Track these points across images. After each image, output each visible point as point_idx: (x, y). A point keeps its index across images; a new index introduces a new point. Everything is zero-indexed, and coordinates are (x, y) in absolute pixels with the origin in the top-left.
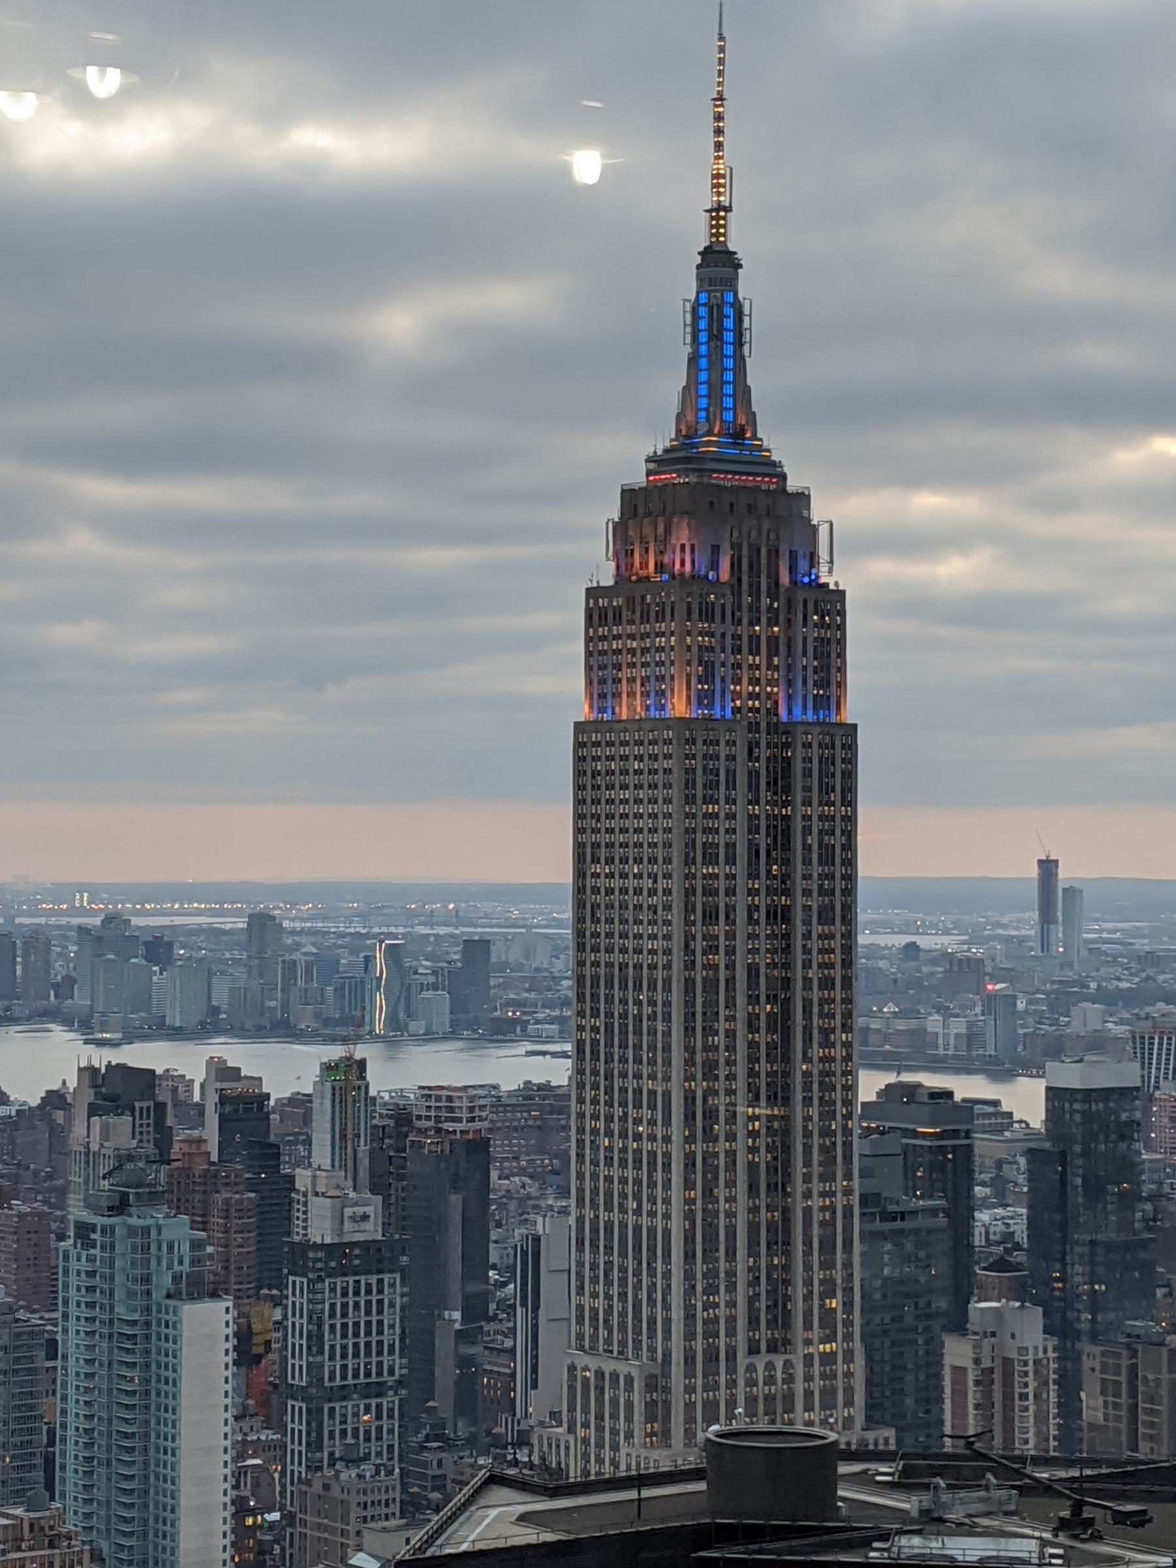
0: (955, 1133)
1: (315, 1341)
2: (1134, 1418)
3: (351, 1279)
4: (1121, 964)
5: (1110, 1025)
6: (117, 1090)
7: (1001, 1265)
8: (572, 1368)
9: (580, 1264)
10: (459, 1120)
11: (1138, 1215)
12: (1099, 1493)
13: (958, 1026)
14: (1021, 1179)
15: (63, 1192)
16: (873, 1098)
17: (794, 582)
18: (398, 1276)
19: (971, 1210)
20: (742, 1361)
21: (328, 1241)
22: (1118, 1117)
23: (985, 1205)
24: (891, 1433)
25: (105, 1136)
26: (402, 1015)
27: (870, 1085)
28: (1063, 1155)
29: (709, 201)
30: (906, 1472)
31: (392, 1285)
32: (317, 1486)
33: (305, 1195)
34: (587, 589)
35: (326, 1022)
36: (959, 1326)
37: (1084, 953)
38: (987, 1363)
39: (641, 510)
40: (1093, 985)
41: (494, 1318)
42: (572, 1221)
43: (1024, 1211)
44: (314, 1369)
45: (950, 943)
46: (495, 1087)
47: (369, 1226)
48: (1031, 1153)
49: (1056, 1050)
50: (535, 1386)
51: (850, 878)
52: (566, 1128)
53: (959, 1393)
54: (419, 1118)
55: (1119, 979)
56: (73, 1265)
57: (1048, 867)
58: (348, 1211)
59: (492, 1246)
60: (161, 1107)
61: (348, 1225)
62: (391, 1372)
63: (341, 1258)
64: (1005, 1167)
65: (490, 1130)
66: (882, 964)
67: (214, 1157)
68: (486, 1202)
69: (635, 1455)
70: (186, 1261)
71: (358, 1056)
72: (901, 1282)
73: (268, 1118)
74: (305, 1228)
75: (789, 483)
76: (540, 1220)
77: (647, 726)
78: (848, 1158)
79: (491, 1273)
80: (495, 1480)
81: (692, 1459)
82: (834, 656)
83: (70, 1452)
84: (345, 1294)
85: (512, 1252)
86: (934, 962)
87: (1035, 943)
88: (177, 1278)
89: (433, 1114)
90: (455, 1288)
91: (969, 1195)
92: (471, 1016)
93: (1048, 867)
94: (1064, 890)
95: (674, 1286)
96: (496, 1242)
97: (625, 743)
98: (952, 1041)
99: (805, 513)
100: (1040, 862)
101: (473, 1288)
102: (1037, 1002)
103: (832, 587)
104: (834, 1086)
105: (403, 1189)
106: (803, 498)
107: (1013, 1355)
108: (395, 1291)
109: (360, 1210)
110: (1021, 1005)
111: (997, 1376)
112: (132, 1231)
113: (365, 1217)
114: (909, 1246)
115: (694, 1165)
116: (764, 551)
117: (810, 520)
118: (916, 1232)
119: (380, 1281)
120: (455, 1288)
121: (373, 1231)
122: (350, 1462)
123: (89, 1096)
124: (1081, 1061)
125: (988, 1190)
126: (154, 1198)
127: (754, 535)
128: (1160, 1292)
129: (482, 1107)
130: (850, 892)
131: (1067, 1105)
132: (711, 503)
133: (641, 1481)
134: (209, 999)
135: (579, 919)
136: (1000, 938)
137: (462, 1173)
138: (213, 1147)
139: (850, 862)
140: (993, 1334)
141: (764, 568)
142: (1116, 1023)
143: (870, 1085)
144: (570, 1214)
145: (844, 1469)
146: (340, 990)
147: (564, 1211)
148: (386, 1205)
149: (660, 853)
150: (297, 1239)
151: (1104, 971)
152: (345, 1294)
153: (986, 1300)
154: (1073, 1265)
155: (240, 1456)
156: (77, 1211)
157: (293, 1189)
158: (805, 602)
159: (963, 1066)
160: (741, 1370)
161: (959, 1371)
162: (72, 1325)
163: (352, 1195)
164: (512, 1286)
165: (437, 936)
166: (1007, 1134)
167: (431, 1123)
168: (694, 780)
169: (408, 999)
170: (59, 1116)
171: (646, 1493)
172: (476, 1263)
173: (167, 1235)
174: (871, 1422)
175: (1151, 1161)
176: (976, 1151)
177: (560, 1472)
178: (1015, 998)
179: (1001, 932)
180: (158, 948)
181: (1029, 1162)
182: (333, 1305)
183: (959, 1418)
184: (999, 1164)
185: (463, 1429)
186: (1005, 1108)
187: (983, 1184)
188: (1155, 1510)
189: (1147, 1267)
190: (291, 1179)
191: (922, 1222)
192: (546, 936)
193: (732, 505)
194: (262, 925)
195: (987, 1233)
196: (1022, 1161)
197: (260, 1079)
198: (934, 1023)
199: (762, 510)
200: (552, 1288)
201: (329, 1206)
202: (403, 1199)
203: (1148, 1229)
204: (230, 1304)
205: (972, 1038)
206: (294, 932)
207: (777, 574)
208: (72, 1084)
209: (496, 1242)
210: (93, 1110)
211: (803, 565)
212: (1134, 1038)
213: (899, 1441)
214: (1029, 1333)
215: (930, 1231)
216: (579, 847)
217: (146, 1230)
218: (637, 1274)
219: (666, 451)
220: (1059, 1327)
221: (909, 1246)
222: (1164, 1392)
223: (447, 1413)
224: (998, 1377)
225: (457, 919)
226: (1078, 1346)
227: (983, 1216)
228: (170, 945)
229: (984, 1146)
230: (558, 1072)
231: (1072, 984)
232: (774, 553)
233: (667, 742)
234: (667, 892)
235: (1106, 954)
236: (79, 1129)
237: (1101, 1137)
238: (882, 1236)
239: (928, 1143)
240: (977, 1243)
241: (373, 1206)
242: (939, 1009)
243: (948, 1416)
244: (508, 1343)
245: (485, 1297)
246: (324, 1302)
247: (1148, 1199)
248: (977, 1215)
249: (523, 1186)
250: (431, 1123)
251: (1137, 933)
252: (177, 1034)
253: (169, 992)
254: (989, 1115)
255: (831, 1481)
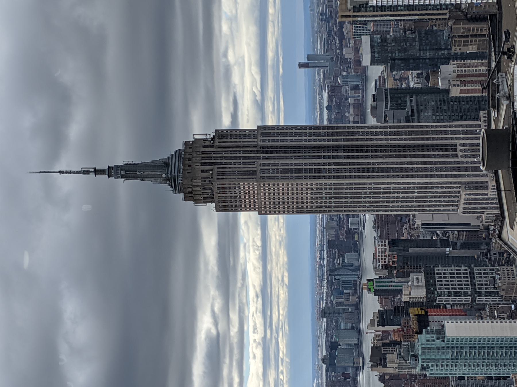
0: (386, 94)
1: (457, 294)
2: (476, 36)
3: (437, 283)
4: (331, 42)
5: (351, 45)
6: (379, 359)
7: (427, 79)
8: (464, 213)
9: (430, 210)
10: (385, 249)
11: (410, 36)
12: (499, 46)
13: (352, 93)
14: (400, 73)
15: (411, 375)
16: (375, 119)
17: (212, 146)
18: (436, 268)
19: (410, 89)
20: (460, 159)
21: (425, 290)
22: (380, 42)
23: (408, 84)
24: (481, 112)
25: (393, 362)
26: (353, 268)
27: (372, 121)
28: (393, 59)
29: (92, 175)
30: (494, 107)
31: (438, 270)
32: (502, 293)
33: (410, 298)
34: (217, 211)
35: (356, 292)
36: (447, 91)
37: (328, 54)
38: (459, 83)
39: (190, 195)
40: (338, 51)
41: (448, 237)
42: (416, 213)
43: (410, 71)
44: (466, 294)
45: (325, 95)
46: (375, 238)
47: (420, 277)
48: (392, 69)
49: (359, 62)
50: (470, 224)
51: (306, 127)
52: (387, 215)
53: (468, 91)
54: (385, 262)
55: (336, 43)
56: (434, 372)
57: (301, 65)
58: (415, 284)
59: (425, 238)
60: (384, 344)
61: (420, 284)
62: (466, 270)
63: (430, 286)
64: (396, 78)
65: (388, 239)
66: (333, 117)
67: (399, 327)
68: (411, 241)
69: (491, 193)
70: (432, 335)
71: (366, 282)
72: (433, 110)
73: (386, 310)
74: (421, 298)
75: (181, 148)
76: (416, 223)
77: (259, 191)
78: (394, 127)
79: (434, 239)
80: (500, 237)
81: (491, 175)
82: (236, 133)
83: (493, 371)
84: (442, 285)
85: (427, 232)
86: (332, 101)
87: (326, 69)
88: (438, 338)
89: (384, 258)
90: (439, 250)
91: (406, 89)
92: (352, 246)
93: (301, 65)
94: (308, 60)
95: (437, 181)
96: (424, 237)
97: (265, 199)
98: (357, 95)
99: (191, 143)
100: (300, 68)
101: (439, 243)
102: (344, 68)
103: (214, 134)
104: (372, 132)
105: (408, 267)
106: (186, 143)
107: (456, 74)
108: (440, 269)
109: (415, 280)
110: (345, 74)
111: (462, 79)
112: (423, 353)
113: (417, 279)
114: (422, 108)
115: (398, 175)
116: (203, 156)
117: (193, 141)
118: (417, 105)
119: (437, 274)
120: (439, 250)
121: (421, 276)
122: (495, 283)
123: (380, 368)
124: (362, 54)
125: (404, 83)
126: (413, 346)
127: (198, 159)
128: (435, 28)
129: (382, 242)
130: (310, 128)
131: (376, 59)
132: (188, 173)
133: (499, 191)
134: (349, 330)
135: (320, 212)
136: (324, 80)
137: (402, 248)
138: (396, 328)
139: (301, 127)
140: (449, 81)
141: (208, 155)
142: (350, 44)
143: (372, 121)
144: (415, 214)
145: (493, 127)
146: (346, 288)
147: (414, 216)
148: (413, 272)
149: (300, 187)
150: (425, 300)
151: (333, 47)
152: (442, 285)
153: (438, 83)
154: (426, 56)
155: (494, 317)
156: (418, 370)
157: (409, 302)
158: (219, 142)
159: (364, 91)
160: (463, 159)
161: (461, 91)
162: (453, 372)
163: (410, 283)
164: (438, 232)
165: (327, 257)
166: (385, 77)
167: (387, 259)
168: (276, 176)
169: (347, 266)
170: (387, 377)
171: (503, 189)
172: (431, 243)
173: (424, 342)
174: (478, 119)
175: (393, 32)
176: (391, 87)
177: (497, 216)
178: (343, 76)
179: (322, 81)
180: (332, 346)
181: (394, 70)
182: (446, 289)
183: (475, 90)
184: (395, 80)
185: (484, 247)
186: (377, 78)
187: (402, 85)
188: (504, 29)
189: (427, 32)
190: (406, 303)
191: (414, 104)
192: (326, 223)
193: (189, 166)
194: (324, 313)
195: (417, 83)
196: (394, 73)
197: (374, 313)
198: (351, 100)
199: (191, 156)
200: (438, 219)
201: (414, 290)
202: (411, 267)
203: (415, 32)
204: (446, 321)
205: (355, 88)
206: (327, 303)
207: (210, 151)
208: (376, 373)
209: (424, 237)
210: (385, 366)
211: (207, 143)
212: (354, 38)
213: (484, 110)
214: (449, 70)
215: (417, 102)
216: (298, 212)
217: (423, 349)
218: (433, 193)
219: (172, 187)
220: (446, 60)
221: (422, 108)
222: (466, 26)
223: (478, 252)
224: (463, 79)
225: (321, 251)
226: (452, 54)
227: (412, 85)
228: (332, 343)
229: (390, 84)
230: (369, 218)
231: (337, 57)
232: (204, 152)
233: (264, 185)
234: (312, 184)
235: (328, 47)
236: (391, 371)
237: (386, 48)
238: (419, 117)
239: (389, 102)
240: (421, 86)
241: (414, 276)
242: (347, 99)
243: (476, 95)
244: (456, 233)
245: (442, 240)
246: (444, 292)
247: (405, 33)
248: (412, 86)
249: (406, 229)
250: (387, 259)
251: (321, 38)
252: (360, 340)
253: (347, 341)
254: (380, 83)
255: (497, 130)
